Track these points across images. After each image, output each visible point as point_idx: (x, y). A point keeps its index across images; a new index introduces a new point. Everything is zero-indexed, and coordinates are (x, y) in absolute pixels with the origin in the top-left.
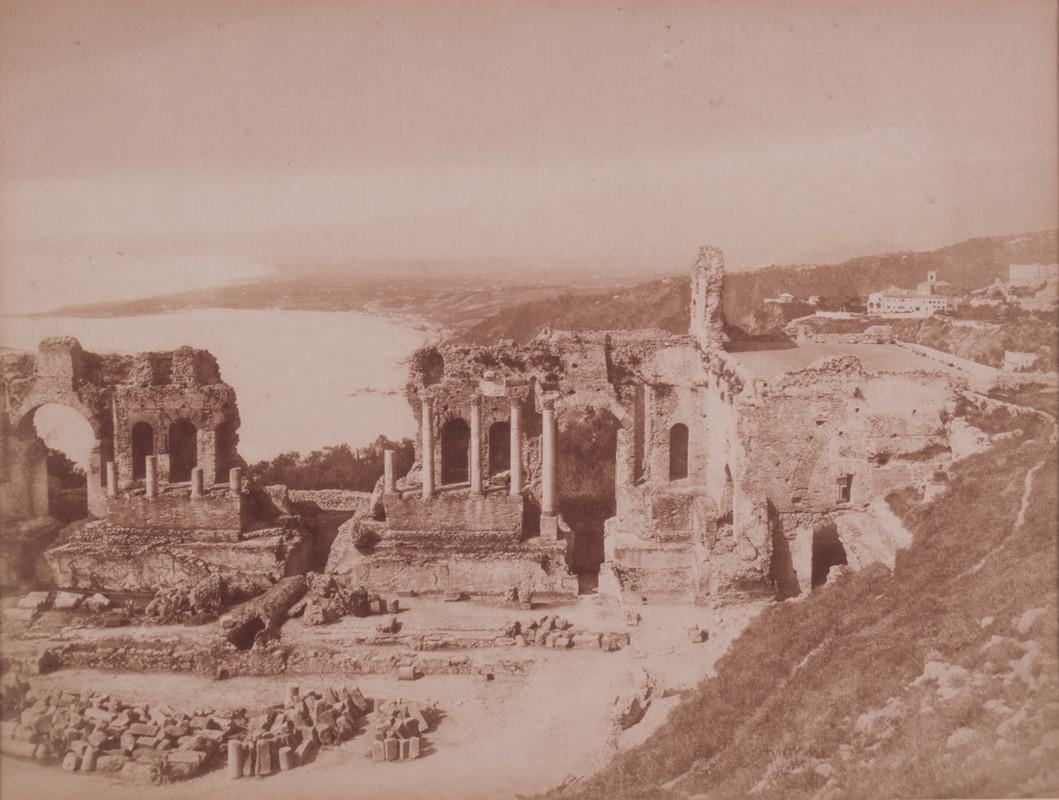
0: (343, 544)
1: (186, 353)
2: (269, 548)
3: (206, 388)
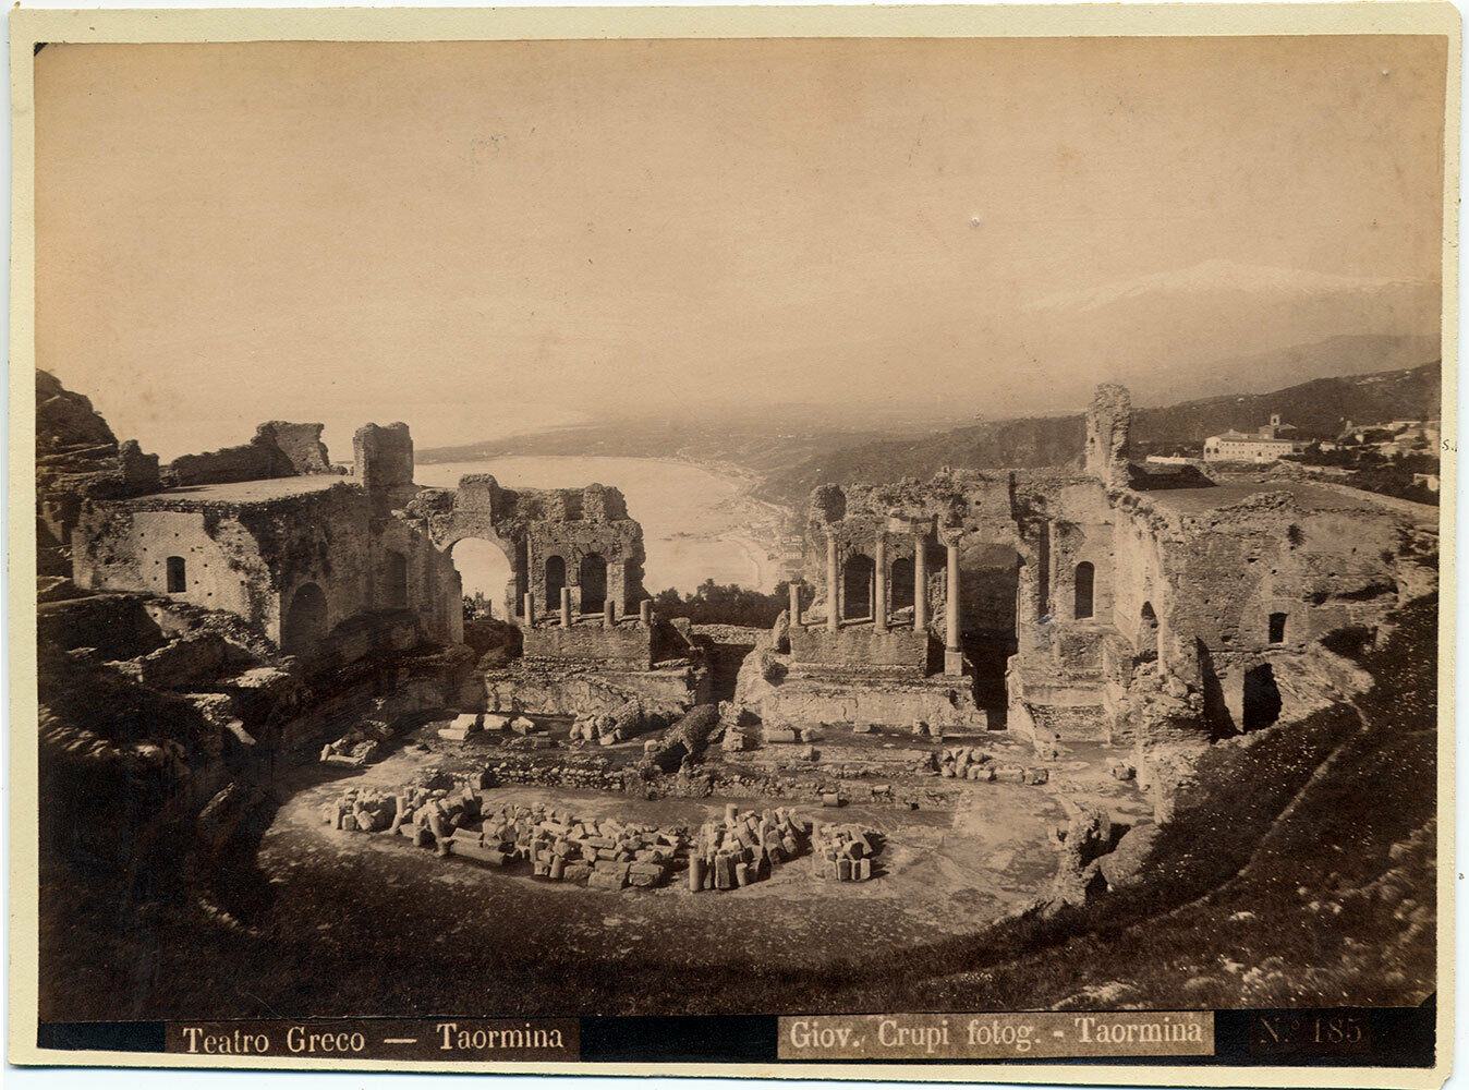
0: (751, 674)
1: (596, 490)
2: (680, 677)
3: (615, 524)
